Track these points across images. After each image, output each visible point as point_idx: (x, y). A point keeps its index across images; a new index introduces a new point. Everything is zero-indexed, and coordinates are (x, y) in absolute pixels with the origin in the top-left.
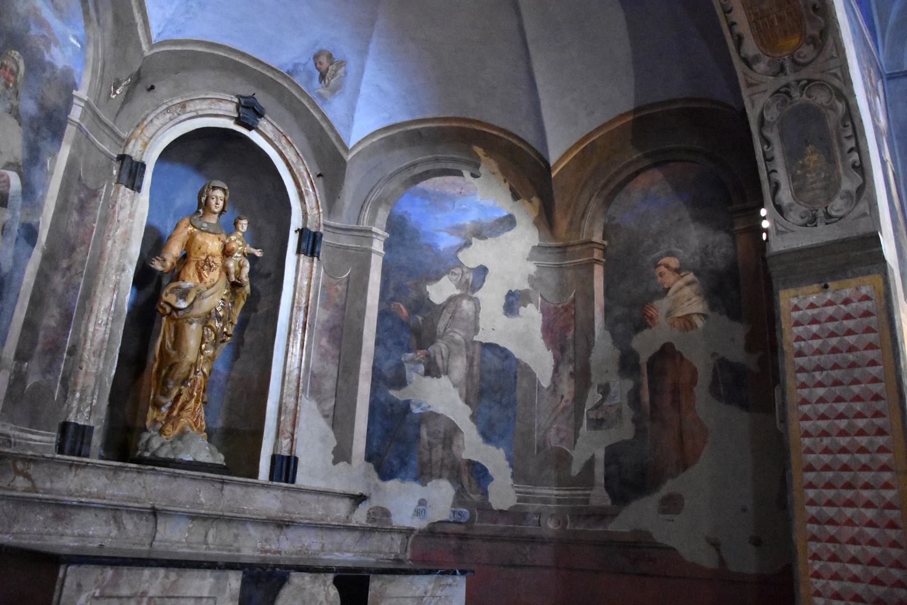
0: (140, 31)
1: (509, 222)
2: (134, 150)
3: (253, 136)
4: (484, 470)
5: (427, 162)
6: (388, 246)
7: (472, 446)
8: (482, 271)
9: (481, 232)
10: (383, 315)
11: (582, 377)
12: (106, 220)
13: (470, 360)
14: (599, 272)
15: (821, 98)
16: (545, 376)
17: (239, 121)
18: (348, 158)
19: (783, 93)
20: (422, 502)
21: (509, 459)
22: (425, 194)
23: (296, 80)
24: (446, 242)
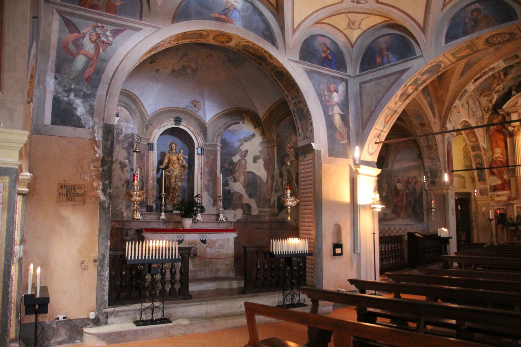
0: (146, 114)
1: (254, 136)
2: (151, 141)
3: (181, 127)
4: (250, 205)
5: (229, 121)
6: (221, 148)
7: (246, 199)
8: (247, 151)
9: (246, 140)
10: (222, 167)
11: (273, 178)
12: (148, 159)
13: (245, 177)
14: (275, 148)
15: (302, 106)
16: (265, 180)
17: (175, 125)
18: (207, 126)
19: (295, 104)
20: (235, 215)
21: (256, 202)
22: (230, 131)
23: (189, 109)
24: (236, 144)
